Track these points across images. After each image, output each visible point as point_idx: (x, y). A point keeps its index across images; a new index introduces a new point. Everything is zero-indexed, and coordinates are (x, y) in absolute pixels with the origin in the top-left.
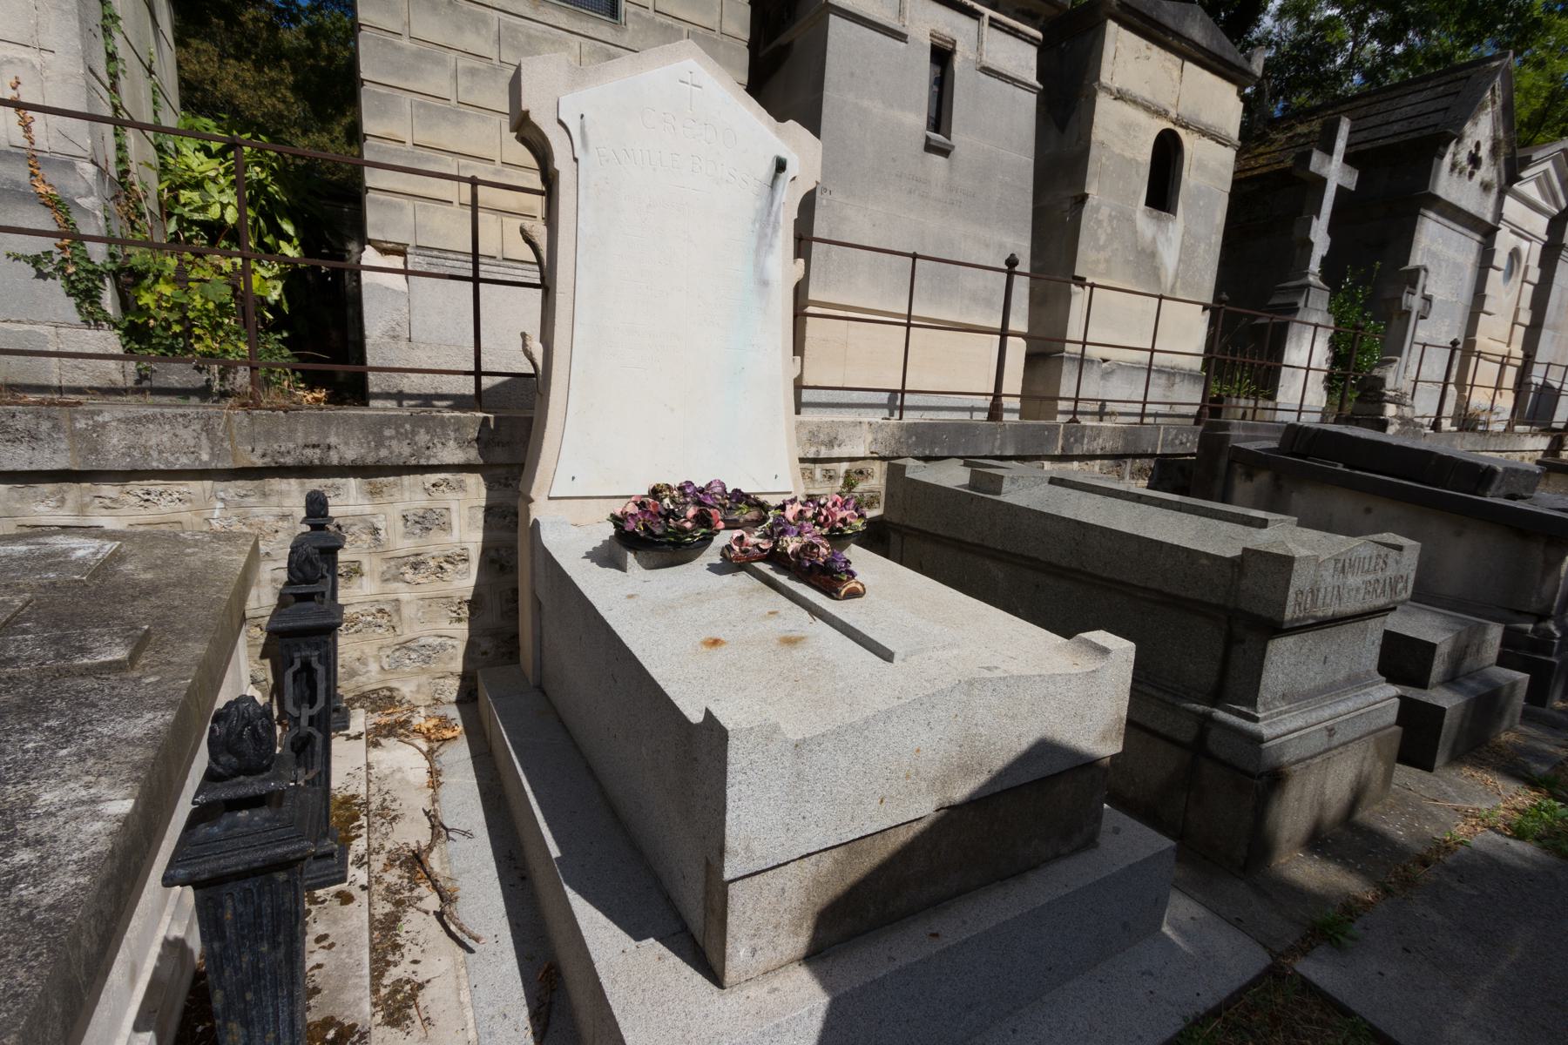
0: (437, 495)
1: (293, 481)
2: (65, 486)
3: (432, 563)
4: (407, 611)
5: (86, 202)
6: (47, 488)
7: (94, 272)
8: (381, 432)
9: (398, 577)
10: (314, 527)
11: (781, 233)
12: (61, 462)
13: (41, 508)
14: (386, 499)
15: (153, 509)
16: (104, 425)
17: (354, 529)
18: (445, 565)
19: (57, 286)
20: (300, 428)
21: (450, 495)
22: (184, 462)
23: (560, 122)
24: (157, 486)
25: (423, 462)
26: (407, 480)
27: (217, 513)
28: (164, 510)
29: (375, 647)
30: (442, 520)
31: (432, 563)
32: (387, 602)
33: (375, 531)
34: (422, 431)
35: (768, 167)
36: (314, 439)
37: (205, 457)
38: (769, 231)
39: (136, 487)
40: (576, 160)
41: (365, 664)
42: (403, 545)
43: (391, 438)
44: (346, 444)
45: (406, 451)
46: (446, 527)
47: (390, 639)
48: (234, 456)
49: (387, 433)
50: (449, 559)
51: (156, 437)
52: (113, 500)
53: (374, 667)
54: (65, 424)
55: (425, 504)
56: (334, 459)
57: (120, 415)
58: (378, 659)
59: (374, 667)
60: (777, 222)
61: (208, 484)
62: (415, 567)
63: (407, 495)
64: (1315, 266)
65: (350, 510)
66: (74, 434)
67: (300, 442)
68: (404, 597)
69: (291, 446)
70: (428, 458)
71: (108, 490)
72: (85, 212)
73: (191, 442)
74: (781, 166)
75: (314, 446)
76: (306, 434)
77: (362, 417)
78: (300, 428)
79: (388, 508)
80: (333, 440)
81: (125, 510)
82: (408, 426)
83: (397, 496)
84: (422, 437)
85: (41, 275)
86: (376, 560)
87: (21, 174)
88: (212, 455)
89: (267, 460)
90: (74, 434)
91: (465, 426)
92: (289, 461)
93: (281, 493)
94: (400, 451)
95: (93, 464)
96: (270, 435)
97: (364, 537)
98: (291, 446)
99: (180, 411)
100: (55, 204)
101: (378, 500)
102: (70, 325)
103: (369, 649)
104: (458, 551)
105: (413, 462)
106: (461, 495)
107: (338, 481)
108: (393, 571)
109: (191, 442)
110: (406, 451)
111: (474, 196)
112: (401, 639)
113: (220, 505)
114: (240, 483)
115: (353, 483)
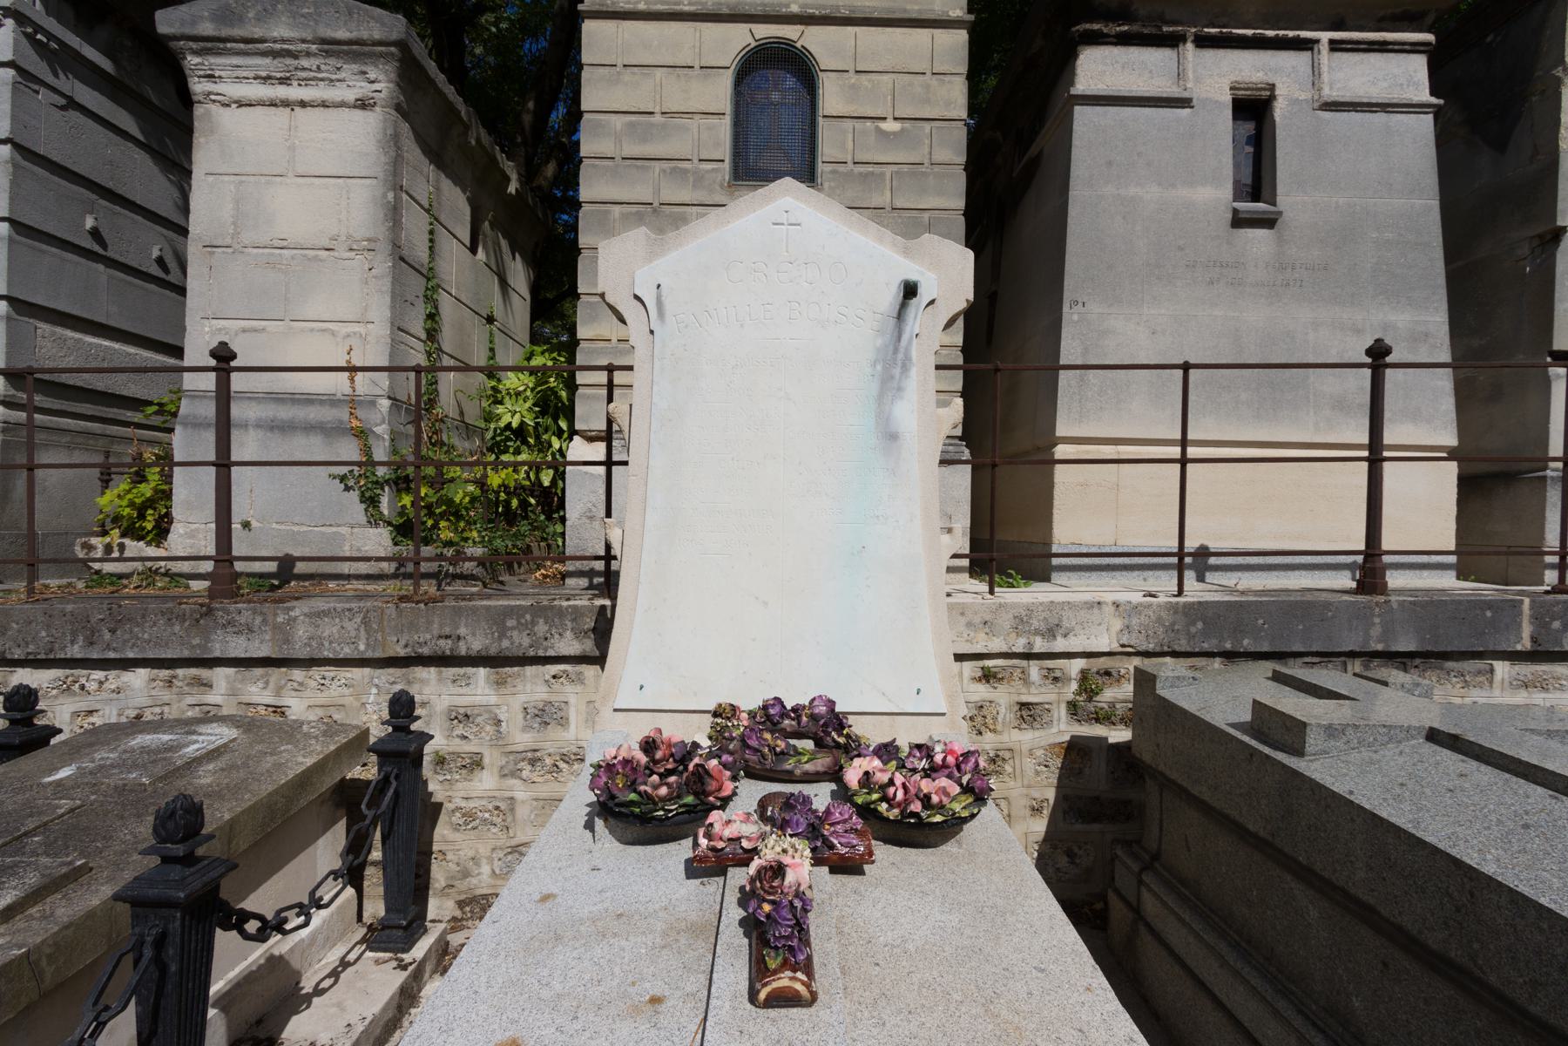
0: (556, 686)
1: (432, 669)
2: (270, 670)
3: (548, 761)
4: (522, 812)
5: (379, 430)
6: (258, 671)
7: (377, 482)
8: (504, 622)
9: (515, 774)
10: (396, 729)
11: (914, 372)
12: (263, 651)
13: (253, 689)
14: (509, 690)
15: (325, 694)
16: (295, 619)
17: (479, 720)
18: (562, 765)
19: (354, 496)
20: (436, 620)
21: (569, 688)
22: (347, 652)
23: (637, 297)
24: (330, 672)
25: (541, 653)
26: (530, 670)
27: (372, 698)
28: (334, 694)
29: (489, 848)
30: (560, 714)
31: (548, 761)
32: (504, 799)
33: (498, 722)
34: (541, 621)
35: (893, 294)
36: (447, 630)
37: (362, 647)
38: (897, 371)
39: (316, 672)
40: (652, 332)
41: (478, 865)
42: (522, 739)
43: (513, 628)
44: (474, 635)
45: (526, 641)
46: (563, 722)
47: (503, 840)
48: (384, 646)
49: (510, 623)
50: (564, 758)
51: (329, 629)
52: (301, 684)
53: (486, 869)
54: (270, 618)
55: (545, 696)
56: (462, 650)
57: (306, 610)
58: (490, 860)
59: (486, 869)
60: (907, 358)
61: (367, 671)
62: (533, 762)
63: (528, 687)
64: (1088, 26)
65: (478, 700)
66: (276, 628)
67: (436, 633)
68: (520, 795)
69: (428, 636)
70: (546, 649)
71: (298, 674)
72: (378, 437)
73: (353, 634)
74: (910, 290)
75: (447, 637)
76: (441, 626)
77: (488, 608)
78: (436, 620)
79: (510, 699)
80: (462, 631)
81: (308, 693)
82: (528, 617)
83: (520, 687)
84: (541, 628)
85: (347, 489)
86: (496, 753)
87: (343, 414)
88: (368, 645)
89: (409, 649)
90: (276, 628)
91: (582, 615)
92: (425, 651)
93: (422, 681)
94: (519, 641)
95: (284, 654)
96: (413, 627)
97: (488, 728)
98: (428, 636)
99: (347, 606)
100: (362, 434)
101: (503, 691)
102: (360, 526)
103: (484, 850)
104: (575, 750)
105: (532, 653)
106: (579, 688)
107: (470, 670)
108: (511, 767)
109: (353, 634)
110: (526, 641)
111: (610, 381)
112: (514, 842)
113: (374, 691)
114: (391, 670)
115: (482, 672)
